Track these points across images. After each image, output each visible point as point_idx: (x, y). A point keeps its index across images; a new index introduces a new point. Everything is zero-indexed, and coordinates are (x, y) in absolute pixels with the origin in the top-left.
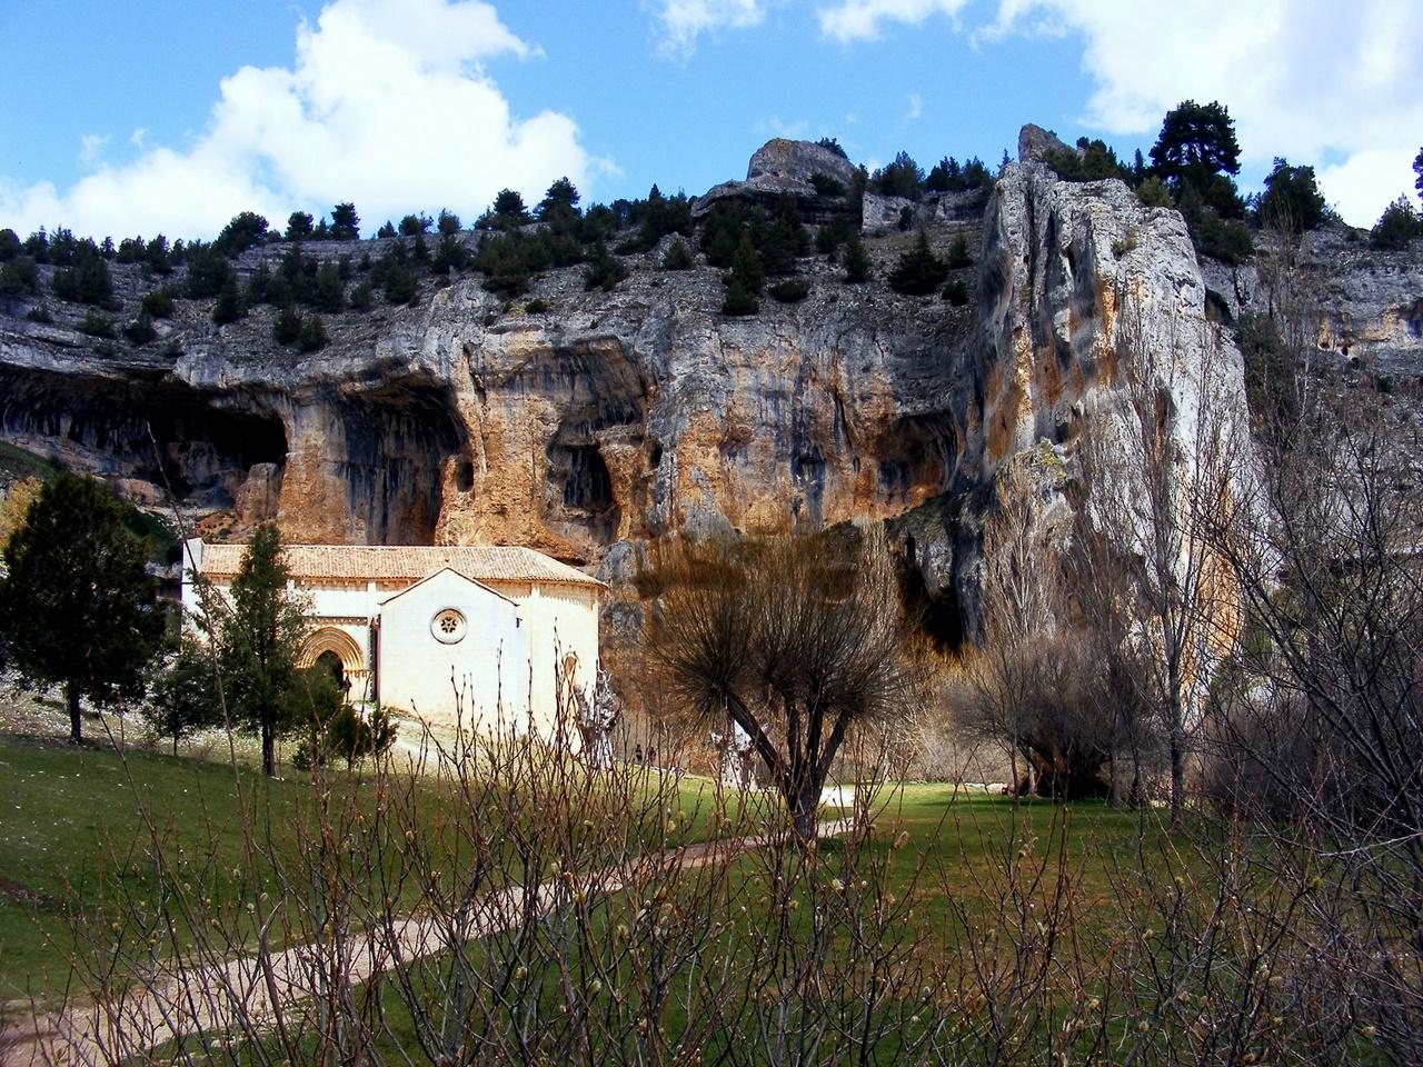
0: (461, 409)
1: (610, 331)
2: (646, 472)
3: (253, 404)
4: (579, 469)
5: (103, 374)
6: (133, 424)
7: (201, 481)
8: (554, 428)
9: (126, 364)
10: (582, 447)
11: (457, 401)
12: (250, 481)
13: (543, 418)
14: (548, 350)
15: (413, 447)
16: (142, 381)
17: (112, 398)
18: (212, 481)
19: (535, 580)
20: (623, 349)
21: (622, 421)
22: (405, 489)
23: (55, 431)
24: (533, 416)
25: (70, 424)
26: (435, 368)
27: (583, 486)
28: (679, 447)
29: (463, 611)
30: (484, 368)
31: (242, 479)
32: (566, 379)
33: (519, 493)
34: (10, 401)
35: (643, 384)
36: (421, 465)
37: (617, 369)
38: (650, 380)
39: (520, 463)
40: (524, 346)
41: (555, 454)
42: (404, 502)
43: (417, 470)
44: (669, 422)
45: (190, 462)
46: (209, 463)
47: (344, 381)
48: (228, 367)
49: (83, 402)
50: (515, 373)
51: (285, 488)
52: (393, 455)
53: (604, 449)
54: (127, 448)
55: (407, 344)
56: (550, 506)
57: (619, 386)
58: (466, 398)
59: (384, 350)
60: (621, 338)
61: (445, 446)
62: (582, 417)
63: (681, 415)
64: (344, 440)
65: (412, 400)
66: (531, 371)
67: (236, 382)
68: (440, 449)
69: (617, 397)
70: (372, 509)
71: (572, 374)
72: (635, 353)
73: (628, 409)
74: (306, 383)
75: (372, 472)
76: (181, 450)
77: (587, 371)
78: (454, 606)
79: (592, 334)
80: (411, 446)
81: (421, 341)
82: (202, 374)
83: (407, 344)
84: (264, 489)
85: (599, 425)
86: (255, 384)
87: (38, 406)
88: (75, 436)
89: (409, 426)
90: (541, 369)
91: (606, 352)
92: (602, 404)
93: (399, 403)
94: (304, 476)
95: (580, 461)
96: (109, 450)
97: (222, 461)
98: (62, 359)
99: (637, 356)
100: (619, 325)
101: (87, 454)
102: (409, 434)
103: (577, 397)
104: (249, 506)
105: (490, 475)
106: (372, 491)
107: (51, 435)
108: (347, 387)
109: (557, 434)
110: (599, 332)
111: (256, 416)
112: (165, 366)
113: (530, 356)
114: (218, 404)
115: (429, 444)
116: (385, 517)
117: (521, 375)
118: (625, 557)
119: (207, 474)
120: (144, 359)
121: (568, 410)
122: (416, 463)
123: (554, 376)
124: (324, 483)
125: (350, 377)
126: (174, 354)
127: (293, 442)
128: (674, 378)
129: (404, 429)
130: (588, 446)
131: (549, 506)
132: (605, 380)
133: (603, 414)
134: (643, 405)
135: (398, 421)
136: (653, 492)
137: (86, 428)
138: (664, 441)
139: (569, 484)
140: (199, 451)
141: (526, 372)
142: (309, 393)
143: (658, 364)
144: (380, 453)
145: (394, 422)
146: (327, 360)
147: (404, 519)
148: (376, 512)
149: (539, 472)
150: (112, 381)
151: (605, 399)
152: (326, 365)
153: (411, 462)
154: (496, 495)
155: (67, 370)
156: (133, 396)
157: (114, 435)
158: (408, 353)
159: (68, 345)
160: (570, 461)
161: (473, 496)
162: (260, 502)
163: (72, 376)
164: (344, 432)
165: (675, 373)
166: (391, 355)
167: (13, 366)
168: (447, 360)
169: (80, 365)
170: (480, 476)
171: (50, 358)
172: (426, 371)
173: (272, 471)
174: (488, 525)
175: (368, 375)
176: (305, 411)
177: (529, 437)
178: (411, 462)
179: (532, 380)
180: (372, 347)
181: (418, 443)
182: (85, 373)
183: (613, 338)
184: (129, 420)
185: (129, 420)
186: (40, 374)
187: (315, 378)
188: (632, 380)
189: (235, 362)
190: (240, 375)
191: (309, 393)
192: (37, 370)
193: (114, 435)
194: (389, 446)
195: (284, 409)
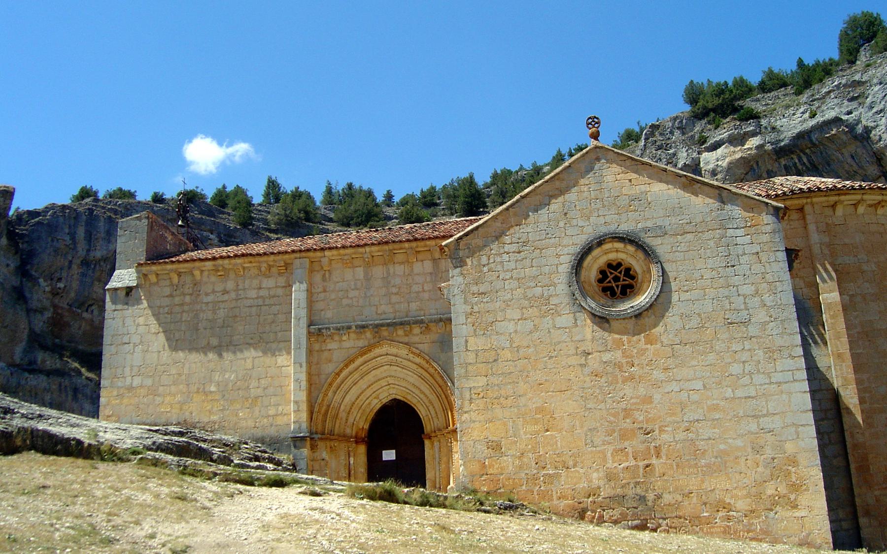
1: (830, 115)
37: (846, 154)
60: (845, 117)
72: (866, 127)
79: (812, 123)
91: (832, 139)
99: (868, 130)
100: (840, 105)
110: (819, 119)
183: (837, 121)
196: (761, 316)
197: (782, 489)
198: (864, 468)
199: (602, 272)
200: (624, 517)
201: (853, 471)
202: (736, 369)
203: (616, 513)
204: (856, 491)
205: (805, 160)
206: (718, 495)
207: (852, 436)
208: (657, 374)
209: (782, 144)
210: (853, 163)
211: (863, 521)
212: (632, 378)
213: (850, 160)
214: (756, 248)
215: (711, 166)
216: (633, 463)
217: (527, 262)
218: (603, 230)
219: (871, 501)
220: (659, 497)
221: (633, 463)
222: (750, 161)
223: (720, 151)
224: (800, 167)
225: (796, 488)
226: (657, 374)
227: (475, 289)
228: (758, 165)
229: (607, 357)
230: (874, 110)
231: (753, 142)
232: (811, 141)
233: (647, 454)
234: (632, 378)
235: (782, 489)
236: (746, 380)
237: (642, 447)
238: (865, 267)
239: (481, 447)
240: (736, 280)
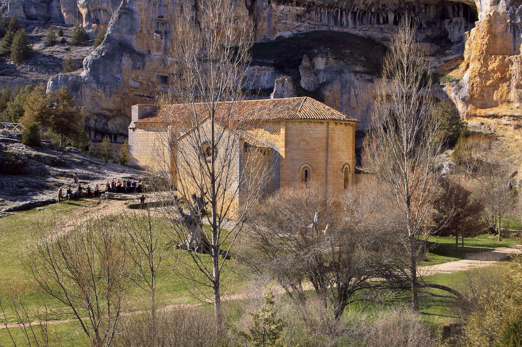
6: (426, 12)
23: (386, 21)
25: (393, 17)
34: (357, 9)
45: (452, 30)
54: (424, 26)
87: (373, 10)
96: (415, 27)
107: (384, 23)
119: (459, 36)
157: (417, 19)
184: (423, 11)
185: (423, 11)
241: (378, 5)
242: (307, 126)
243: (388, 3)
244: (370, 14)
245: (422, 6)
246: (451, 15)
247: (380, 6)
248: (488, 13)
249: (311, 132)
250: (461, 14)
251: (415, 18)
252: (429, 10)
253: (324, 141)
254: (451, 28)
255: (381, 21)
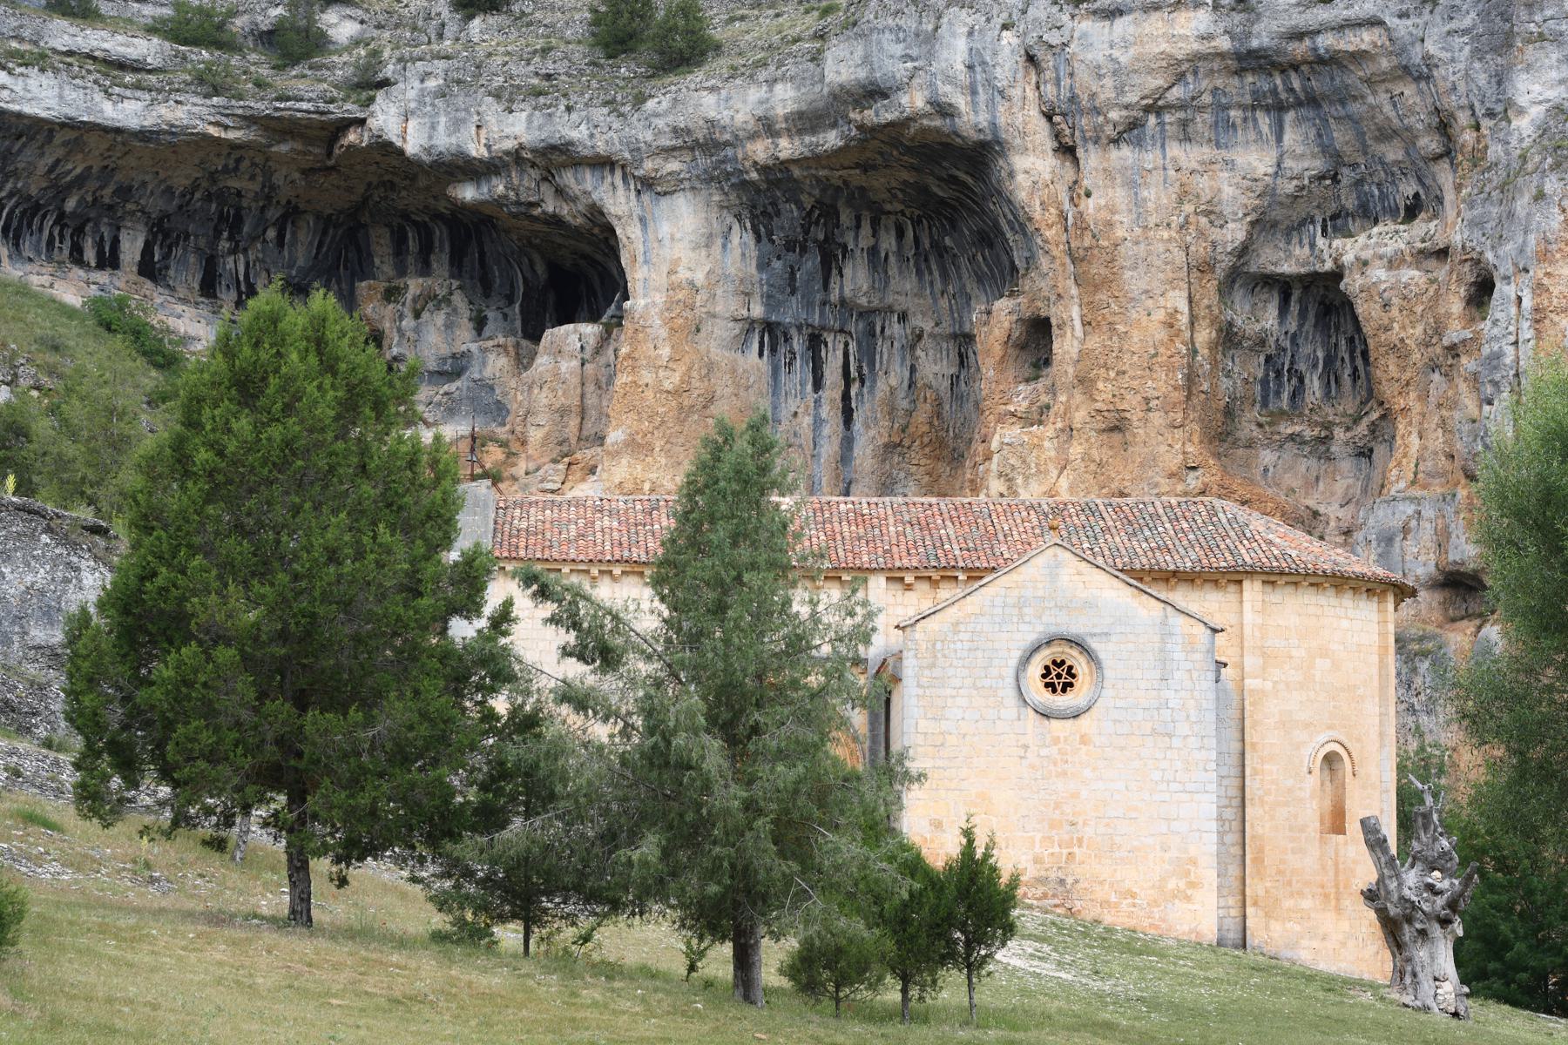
0: (1022, 196)
2: (1456, 332)
3: (547, 191)
4: (1293, 326)
5: (213, 131)
7: (432, 365)
8: (1235, 233)
9: (261, 107)
10: (1300, 278)
11: (1011, 175)
12: (543, 362)
13: (1211, 212)
14: (1222, 55)
15: (910, 284)
16: (298, 146)
17: (234, 183)
18: (454, 367)
19: (1251, 573)
20: (1398, 48)
21: (1394, 212)
22: (892, 377)
24: (1188, 208)
25: (140, 243)
26: (961, 102)
27: (1302, 367)
28: (1537, 272)
29: (1094, 644)
30: (1073, 99)
31: (523, 362)
32: (1264, 121)
33: (1163, 384)
34: (11, 195)
35: (1444, 126)
36: (928, 326)
38: (1463, 118)
39: (1160, 315)
40: (1164, 46)
41: (1238, 294)
42: (892, 412)
43: (920, 337)
44: (1511, 215)
46: (449, 326)
47: (753, 136)
48: (491, 109)
49: (169, 191)
50: (1147, 110)
51: (622, 379)
52: (863, 301)
53: (1352, 283)
55: (898, 49)
56: (1229, 412)
57: (1387, 134)
58: (1031, 170)
59: (843, 65)
60: (1392, 21)
61: (980, 280)
62: (1302, 209)
63: (1540, 196)
64: (753, 269)
65: (905, 175)
66: (1182, 106)
67: (509, 145)
68: (971, 286)
69: (1383, 163)
70: (818, 423)
71: (1279, 108)
72: (1427, 57)
73: (1409, 188)
74: (666, 142)
75: (815, 342)
76: (391, 294)
77: (1312, 101)
78: (1075, 628)
80: (904, 288)
81: (930, 39)
82: (433, 127)
83: (898, 49)
84: (575, 380)
85: (1337, 223)
86: (554, 148)
87: (71, 204)
88: (149, 269)
89: (900, 234)
90: (1207, 99)
91: (1359, 56)
92: (1347, 176)
93: (878, 183)
94: (665, 351)
95: (1294, 308)
97: (480, 324)
98: (123, 98)
101: (179, 308)
102: (900, 252)
103: (1288, 163)
104: (542, 419)
105: (1094, 342)
106: (818, 385)
107: (100, 266)
108: (760, 150)
109: (1244, 251)
111: (555, 221)
112: (351, 109)
113: (1180, 70)
114: (468, 193)
115: (945, 276)
116: (848, 443)
117: (1158, 114)
118: (1405, 530)
119: (445, 350)
120: (307, 92)
121: (1268, 192)
122: (917, 321)
123: (1234, 114)
124: (711, 367)
125: (767, 127)
126: (370, 84)
127: (638, 276)
128: (1521, 112)
129: (888, 242)
130: (1315, 276)
131: (1229, 412)
132: (1354, 120)
133: (1350, 203)
134: (1444, 176)
135: (875, 224)
136: (1475, 378)
137: (178, 252)
138: (1500, 259)
139: (1268, 359)
140: (427, 301)
141: (1169, 107)
142: (674, 165)
143: (1482, 79)
144: (834, 296)
145: (866, 229)
146: (712, 89)
147: (891, 448)
148: (826, 430)
149: (1204, 335)
150: (234, 146)
151: (1354, 166)
152: (720, 101)
153: (903, 317)
154: (1104, 389)
155: (134, 123)
156: (278, 179)
158: (901, 70)
159: (136, 67)
160: (1272, 312)
161: (1052, 390)
162: (563, 412)
163: (144, 135)
164: (752, 250)
165: (1522, 100)
166: (862, 74)
167: (19, 115)
168: (989, 82)
169: (163, 110)
170: (1066, 346)
171: (99, 97)
172: (943, 110)
173: (592, 342)
174: (1086, 457)
175: (805, 121)
176: (665, 202)
177: (1179, 257)
178: (903, 317)
179: (1184, 124)
180: (816, 57)
181: (919, 273)
182: (173, 131)
183: (1374, 22)
184: (271, 234)
186: (77, 132)
187: (688, 131)
188: (1420, 120)
189: (507, 97)
190: (516, 128)
191: (674, 165)
192: (70, 125)
193: (233, 265)
194: (855, 281)
195: (617, 201)
196: (1183, 729)
197: (1182, 885)
198: (1259, 860)
199: (1047, 668)
200: (1045, 896)
201: (1248, 861)
202: (1157, 776)
203: (1039, 893)
204: (1248, 882)
205: (1296, 84)
206: (1127, 884)
207: (1252, 826)
208: (1087, 773)
209: (1255, 43)
210: (1392, 114)
211: (1250, 910)
212: (1065, 774)
213: (1387, 108)
214: (1189, 665)
215: (1097, 55)
216: (1057, 849)
217: (979, 654)
218: (1053, 630)
219: (1261, 893)
220: (1077, 881)
221: (1057, 849)
222: (1179, 62)
223: (1122, 25)
224: (1283, 96)
225: (1192, 885)
226: (1087, 773)
227: (927, 672)
228: (1195, 73)
229: (1044, 752)
230: (1453, 25)
231: (1193, 24)
232: (1315, 49)
233: (1070, 844)
234: (1065, 774)
235: (1182, 885)
236: (1163, 787)
237: (1066, 837)
238: (1294, 653)
239: (925, 823)
240: (1170, 694)
241: (102, 188)
242: (1334, 601)
243: (144, 184)
244: (49, 223)
245: (273, 214)
246: (383, 262)
247: (108, 191)
248: (683, 274)
249: (1345, 624)
250: (441, 262)
251: (231, 259)
252: (294, 234)
253: (1375, 659)
254: (401, 317)
255: (90, 255)
